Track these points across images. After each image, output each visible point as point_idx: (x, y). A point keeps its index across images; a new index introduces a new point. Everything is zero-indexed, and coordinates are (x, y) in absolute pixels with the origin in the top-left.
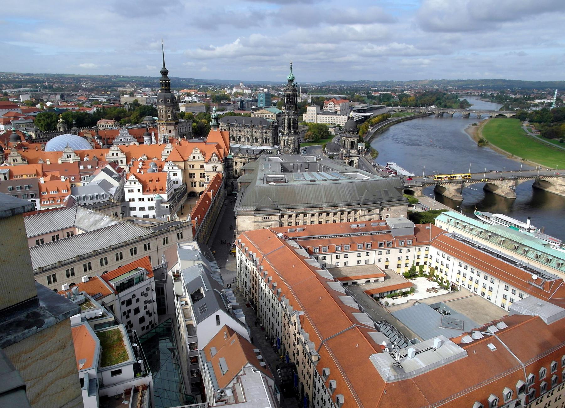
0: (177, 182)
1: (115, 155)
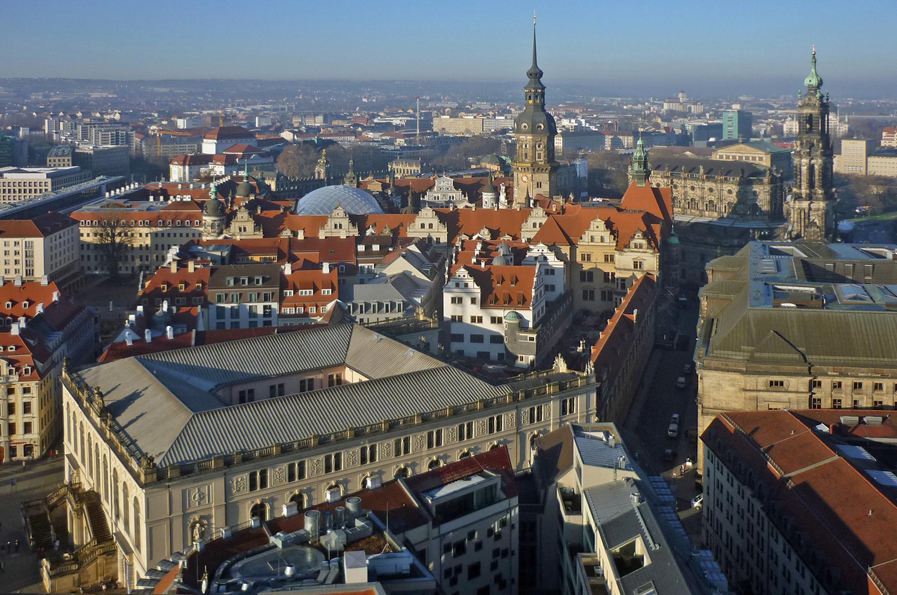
0: (553, 288)
1: (427, 226)
